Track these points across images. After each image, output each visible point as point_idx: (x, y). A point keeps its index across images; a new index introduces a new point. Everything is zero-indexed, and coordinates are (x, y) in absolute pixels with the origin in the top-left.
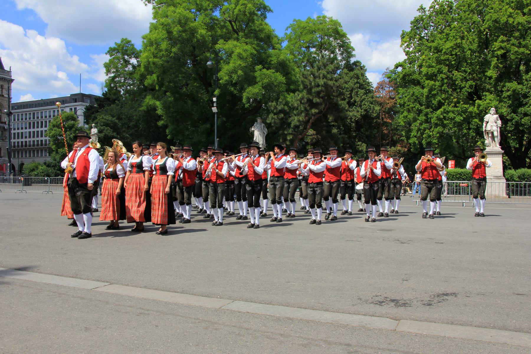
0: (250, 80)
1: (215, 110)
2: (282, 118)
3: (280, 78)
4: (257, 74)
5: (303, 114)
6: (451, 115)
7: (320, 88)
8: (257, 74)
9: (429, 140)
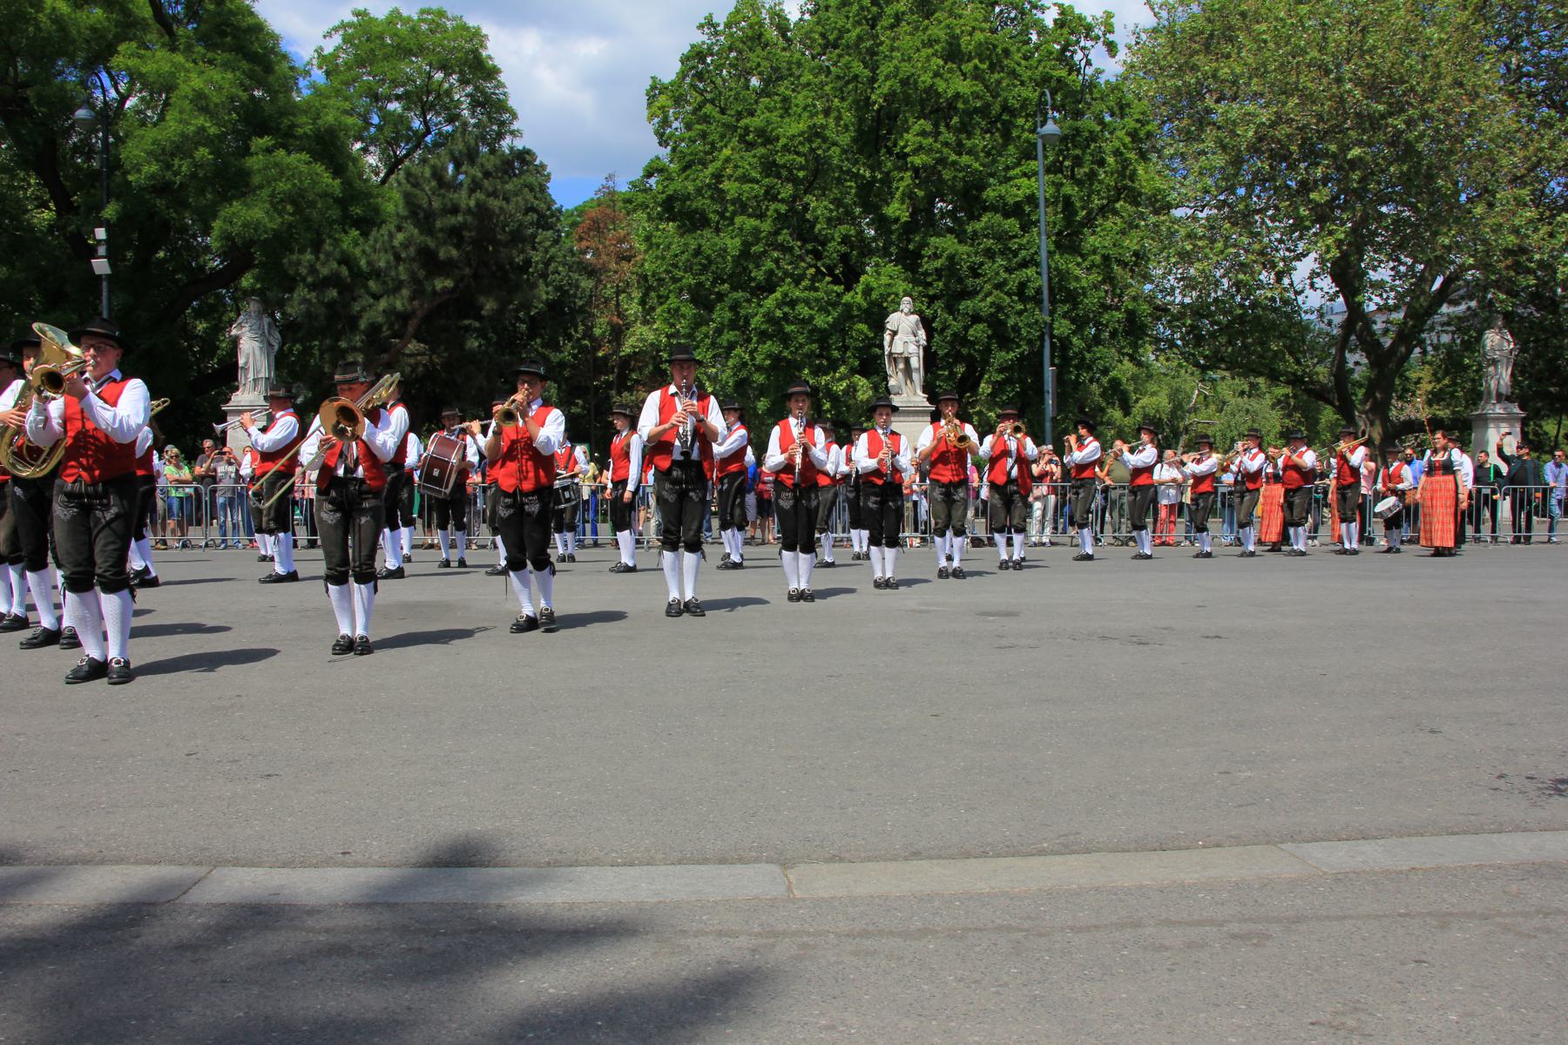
0: (230, 181)
1: (101, 266)
2: (331, 305)
3: (329, 181)
4: (255, 162)
5: (405, 292)
6: (804, 311)
7: (460, 218)
8: (255, 162)
9: (743, 374)
